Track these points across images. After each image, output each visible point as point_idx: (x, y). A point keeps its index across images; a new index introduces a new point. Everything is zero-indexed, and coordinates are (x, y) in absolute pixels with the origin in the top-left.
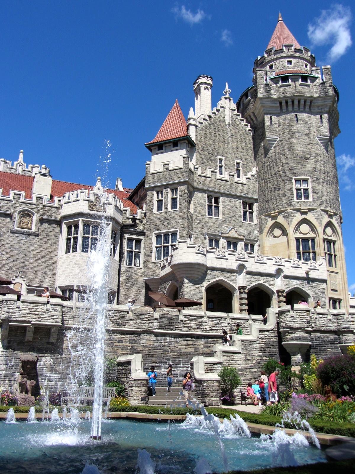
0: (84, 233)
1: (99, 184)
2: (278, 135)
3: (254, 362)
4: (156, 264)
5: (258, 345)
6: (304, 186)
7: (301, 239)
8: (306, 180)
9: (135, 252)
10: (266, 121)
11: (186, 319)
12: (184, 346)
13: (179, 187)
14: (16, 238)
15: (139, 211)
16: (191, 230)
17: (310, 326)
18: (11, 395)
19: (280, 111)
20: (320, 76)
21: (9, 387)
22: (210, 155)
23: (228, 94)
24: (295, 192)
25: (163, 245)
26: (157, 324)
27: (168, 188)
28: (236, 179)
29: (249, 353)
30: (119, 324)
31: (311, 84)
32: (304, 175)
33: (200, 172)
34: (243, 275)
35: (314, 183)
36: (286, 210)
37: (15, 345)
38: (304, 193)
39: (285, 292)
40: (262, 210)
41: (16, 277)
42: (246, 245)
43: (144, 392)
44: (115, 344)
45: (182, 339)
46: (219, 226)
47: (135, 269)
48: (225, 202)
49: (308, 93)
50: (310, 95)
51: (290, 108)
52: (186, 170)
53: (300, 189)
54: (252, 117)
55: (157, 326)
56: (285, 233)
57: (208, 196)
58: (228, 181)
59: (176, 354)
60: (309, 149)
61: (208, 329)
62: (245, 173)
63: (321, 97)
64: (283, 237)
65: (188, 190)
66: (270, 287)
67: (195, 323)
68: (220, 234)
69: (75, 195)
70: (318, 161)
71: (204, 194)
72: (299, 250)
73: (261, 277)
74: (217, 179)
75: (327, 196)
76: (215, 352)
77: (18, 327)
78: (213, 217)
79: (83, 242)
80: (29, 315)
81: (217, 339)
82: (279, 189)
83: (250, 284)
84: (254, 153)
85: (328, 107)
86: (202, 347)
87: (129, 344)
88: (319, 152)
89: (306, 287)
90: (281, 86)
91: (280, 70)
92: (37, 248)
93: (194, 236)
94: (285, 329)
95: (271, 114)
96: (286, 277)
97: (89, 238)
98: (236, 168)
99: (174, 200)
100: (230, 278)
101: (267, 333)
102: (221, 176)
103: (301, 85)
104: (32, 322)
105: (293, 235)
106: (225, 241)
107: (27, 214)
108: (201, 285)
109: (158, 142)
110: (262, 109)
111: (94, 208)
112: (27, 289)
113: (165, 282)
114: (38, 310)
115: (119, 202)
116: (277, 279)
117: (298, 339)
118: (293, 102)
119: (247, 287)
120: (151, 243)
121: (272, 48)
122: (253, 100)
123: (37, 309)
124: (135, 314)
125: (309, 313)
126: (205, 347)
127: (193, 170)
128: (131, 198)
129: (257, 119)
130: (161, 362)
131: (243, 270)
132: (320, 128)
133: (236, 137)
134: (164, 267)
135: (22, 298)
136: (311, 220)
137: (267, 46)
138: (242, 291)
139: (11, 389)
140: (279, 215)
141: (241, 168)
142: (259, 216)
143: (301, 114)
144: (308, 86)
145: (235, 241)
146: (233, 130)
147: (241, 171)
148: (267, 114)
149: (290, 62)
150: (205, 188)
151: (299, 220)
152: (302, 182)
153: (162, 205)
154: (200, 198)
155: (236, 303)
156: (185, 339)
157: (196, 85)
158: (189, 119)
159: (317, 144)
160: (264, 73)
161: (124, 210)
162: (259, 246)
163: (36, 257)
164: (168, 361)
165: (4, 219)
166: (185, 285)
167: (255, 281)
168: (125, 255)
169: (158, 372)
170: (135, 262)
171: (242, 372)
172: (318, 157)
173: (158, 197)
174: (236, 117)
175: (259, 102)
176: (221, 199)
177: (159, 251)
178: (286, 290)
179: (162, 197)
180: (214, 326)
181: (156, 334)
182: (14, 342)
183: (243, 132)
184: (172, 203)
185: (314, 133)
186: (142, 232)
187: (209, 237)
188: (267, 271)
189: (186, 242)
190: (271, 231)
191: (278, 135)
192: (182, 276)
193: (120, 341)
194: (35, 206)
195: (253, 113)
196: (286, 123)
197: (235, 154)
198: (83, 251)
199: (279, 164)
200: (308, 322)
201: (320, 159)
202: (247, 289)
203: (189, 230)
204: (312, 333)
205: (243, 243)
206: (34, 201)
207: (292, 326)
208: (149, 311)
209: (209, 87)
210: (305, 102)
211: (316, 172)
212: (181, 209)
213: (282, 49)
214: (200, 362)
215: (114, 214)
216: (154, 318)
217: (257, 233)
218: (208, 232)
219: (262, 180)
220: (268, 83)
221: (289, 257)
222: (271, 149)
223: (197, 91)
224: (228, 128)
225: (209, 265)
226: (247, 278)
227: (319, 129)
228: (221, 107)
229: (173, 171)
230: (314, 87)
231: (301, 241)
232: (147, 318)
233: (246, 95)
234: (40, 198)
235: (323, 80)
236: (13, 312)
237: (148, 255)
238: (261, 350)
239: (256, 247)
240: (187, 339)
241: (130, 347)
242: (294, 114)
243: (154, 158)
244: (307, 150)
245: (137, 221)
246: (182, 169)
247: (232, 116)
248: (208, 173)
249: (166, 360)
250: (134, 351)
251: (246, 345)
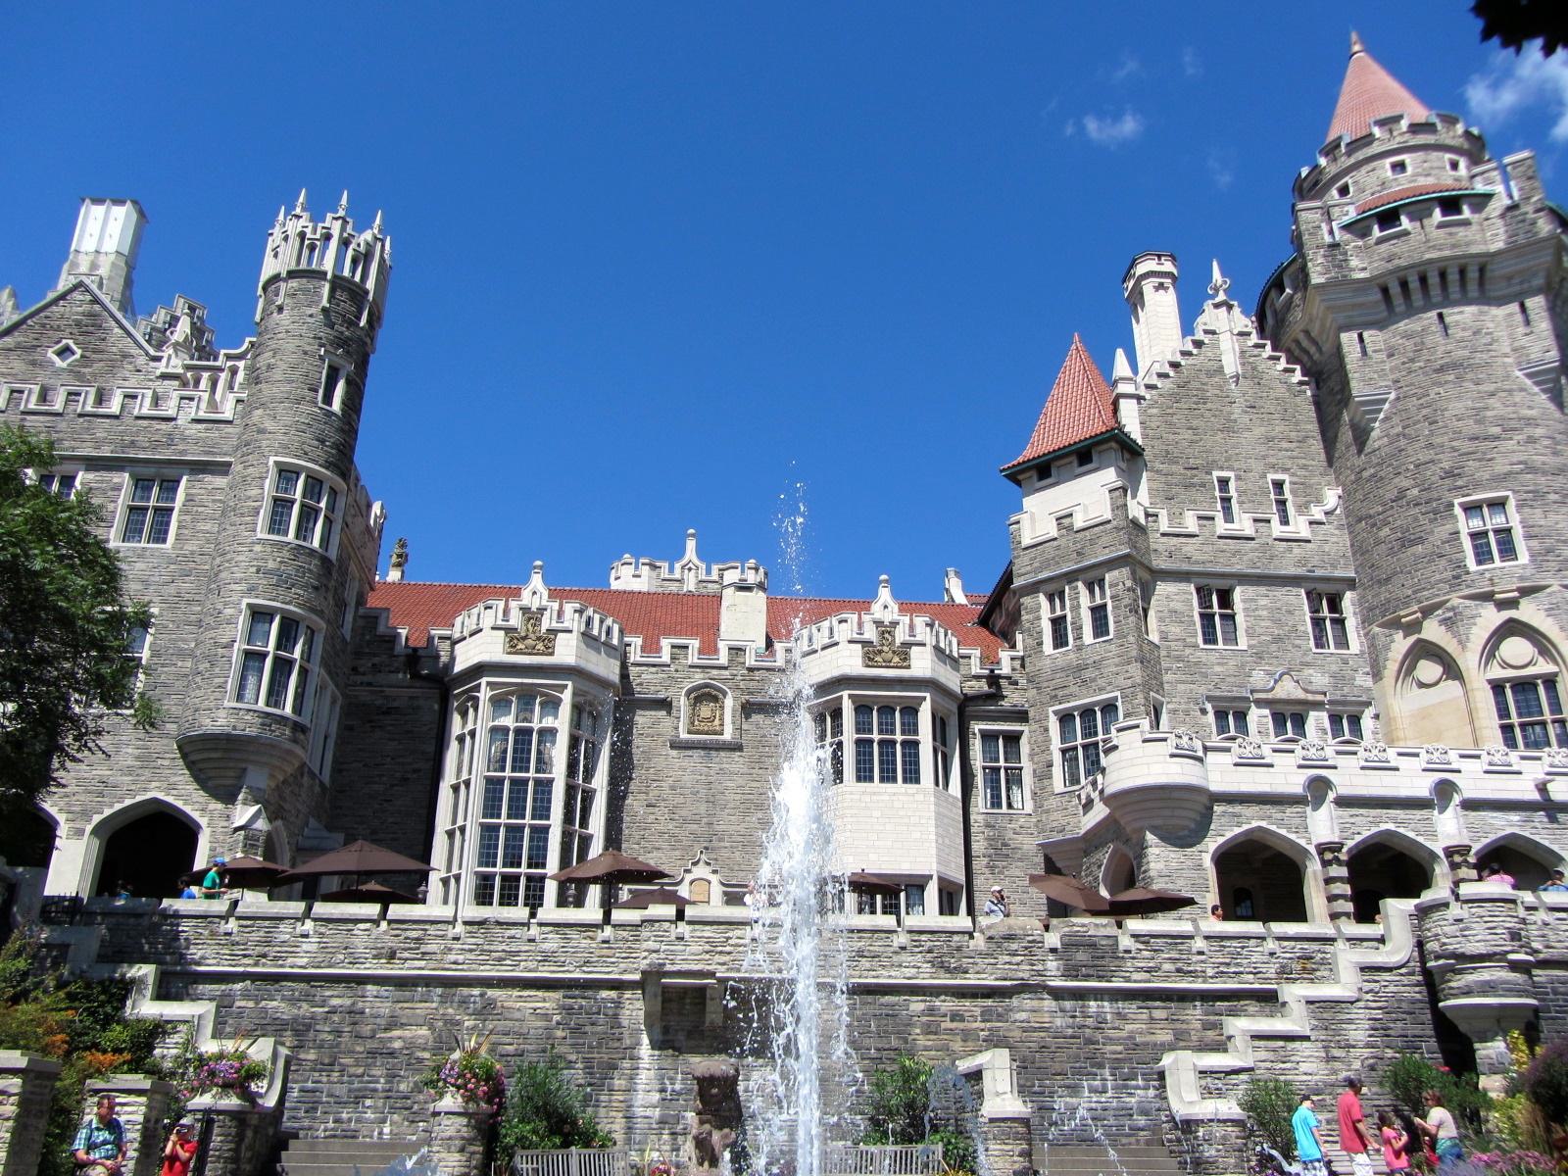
0: (858, 731)
1: (885, 594)
2: (1390, 383)
3: (1357, 1065)
4: (1067, 798)
5: (1363, 1014)
6: (1494, 521)
7: (1508, 685)
8: (1499, 505)
9: (1006, 769)
10: (1345, 349)
11: (1141, 947)
12: (1144, 1026)
13: (1107, 576)
14: (687, 760)
15: (1005, 655)
16: (1157, 692)
17: (1521, 947)
18: (673, 1170)
19: (1385, 314)
20: (1499, 188)
21: (673, 1150)
22: (1189, 473)
23: (1221, 293)
24: (1467, 544)
25: (1080, 741)
26: (1055, 963)
27: (1077, 580)
28: (1277, 529)
29: (1337, 1038)
30: (948, 970)
31: (1475, 218)
32: (1491, 489)
33: (1164, 525)
34: (1327, 809)
35: (1527, 510)
36: (1448, 601)
37: (681, 1037)
38: (1499, 543)
39: (1473, 851)
40: (1371, 609)
41: (695, 864)
42: (1335, 719)
43: (1020, 1155)
44: (943, 1025)
45: (1134, 1006)
46: (1244, 672)
47: (1011, 818)
48: (1252, 600)
49: (1468, 244)
50: (1474, 250)
51: (1417, 298)
52: (1123, 523)
53: (1485, 534)
54: (1305, 343)
55: (1058, 969)
56: (1452, 670)
57: (1198, 590)
58: (1253, 539)
59: (1120, 1048)
60: (1497, 407)
61: (1210, 972)
62: (1303, 508)
63: (1512, 250)
64: (1450, 682)
65: (1134, 580)
66: (1420, 839)
67: (1167, 956)
68: (1249, 695)
69: (826, 633)
70: (1531, 440)
71: (1183, 586)
72: (1509, 716)
73: (1385, 811)
74: (1220, 537)
76: (1230, 1038)
77: (685, 989)
78: (1220, 645)
79: (858, 753)
80: (707, 957)
81: (1242, 1003)
82: (1414, 543)
83: (1354, 833)
84: (1325, 447)
85: (1542, 274)
86: (1198, 1025)
87: (982, 1025)
89: (1545, 831)
90: (1380, 241)
91: (1373, 194)
92: (741, 781)
93: (1169, 706)
94: (1441, 962)
95: (1359, 326)
96: (1470, 805)
97: (871, 741)
98: (1272, 496)
99: (1099, 613)
100: (1285, 822)
101: (1386, 976)
102: (1229, 526)
103: (1441, 226)
104: (718, 975)
105: (1479, 677)
106: (1267, 712)
107: (704, 695)
108: (1199, 847)
109: (1034, 458)
110: (1330, 317)
111: (878, 659)
112: (725, 893)
113: (1096, 848)
114: (730, 942)
115: (946, 636)
116: (1441, 812)
117: (1488, 988)
118: (1423, 280)
119: (1343, 845)
120: (1048, 740)
121: (1340, 138)
122: (1299, 295)
123: (728, 938)
124: (990, 938)
125: (1512, 906)
126: (1208, 1026)
127: (1142, 521)
128: (984, 621)
129: (1320, 350)
130: (1079, 1072)
131: (1327, 794)
132: (1524, 341)
133: (1262, 410)
134: (1088, 805)
135: (689, 911)
136: (1535, 623)
137: (1325, 133)
138: (1328, 856)
139: (677, 1156)
140: (1425, 616)
141: (1287, 495)
142: (1364, 628)
143: (1456, 310)
144: (1466, 223)
145: (1297, 709)
146: (1250, 391)
147: (1289, 505)
148: (1348, 328)
149: (1399, 167)
150: (1185, 567)
151: (1493, 628)
152: (1485, 510)
153: (1066, 628)
154: (1174, 599)
155: (1313, 895)
156: (1144, 1004)
157: (1131, 283)
158: (1116, 381)
159: (1522, 390)
160: (1322, 215)
161: (962, 657)
162: (1377, 717)
163: (742, 806)
164: (1098, 1071)
165: (653, 713)
166: (1150, 850)
167: (1366, 827)
168: (979, 780)
169: (1072, 1104)
170: (1008, 797)
171: (1320, 1097)
172: (1529, 431)
173: (1053, 610)
174: (1256, 351)
175: (1318, 299)
176: (1238, 595)
177: (1071, 759)
178: (1476, 847)
179: (1063, 607)
180: (1228, 964)
181: (1057, 994)
182: (677, 1031)
183: (1281, 391)
184: (1094, 620)
185: (1506, 360)
186: (1020, 712)
187: (1213, 707)
188: (1404, 792)
189: (1138, 727)
190: (1407, 670)
191: (1390, 383)
192: (1137, 825)
193: (956, 1017)
194: (726, 672)
195: (1307, 333)
196: (1409, 344)
197: (1264, 457)
198: (859, 779)
199: (1404, 467)
200: (1515, 936)
201: (1539, 432)
202: (1345, 850)
203: (1151, 693)
204: (1535, 972)
205: (1324, 715)
206: (723, 658)
207: (1460, 950)
208: (1032, 929)
209: (1167, 281)
210: (1462, 272)
211: (1529, 476)
212: (1120, 635)
213: (1371, 135)
214: (1182, 1067)
215: (933, 670)
216: (1047, 946)
217: (1363, 680)
218: (1210, 693)
219: (1360, 520)
220: (1337, 238)
221: (1476, 742)
222: (1373, 429)
223: (1137, 300)
224: (1233, 386)
225: (1214, 787)
226: (1341, 818)
227: (1522, 343)
228: (1206, 332)
229: (1087, 533)
230: (1486, 223)
231: (1509, 692)
232: (1026, 948)
233: (1278, 284)
234: (737, 651)
235: (1511, 196)
236: (668, 950)
237: (1043, 774)
238: (1373, 1029)
239: (1367, 723)
240: (1150, 1004)
241: (987, 1033)
242: (1433, 314)
243: (1030, 502)
244: (1489, 413)
245: (1003, 682)
246: (1109, 522)
247: (1242, 352)
248: (1191, 523)
249: (1092, 1067)
250: (995, 1041)
251: (1325, 1015)
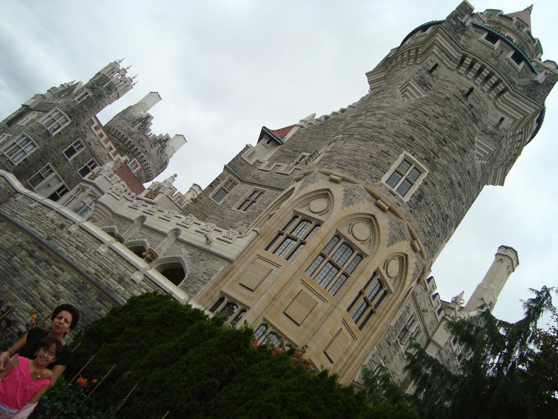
22: (293, 152)
58: (288, 175)
74: (277, 173)
75: (349, 155)
88: (385, 105)
150: (255, 181)
172: (377, 112)
188: (162, 230)
201: (382, 112)
